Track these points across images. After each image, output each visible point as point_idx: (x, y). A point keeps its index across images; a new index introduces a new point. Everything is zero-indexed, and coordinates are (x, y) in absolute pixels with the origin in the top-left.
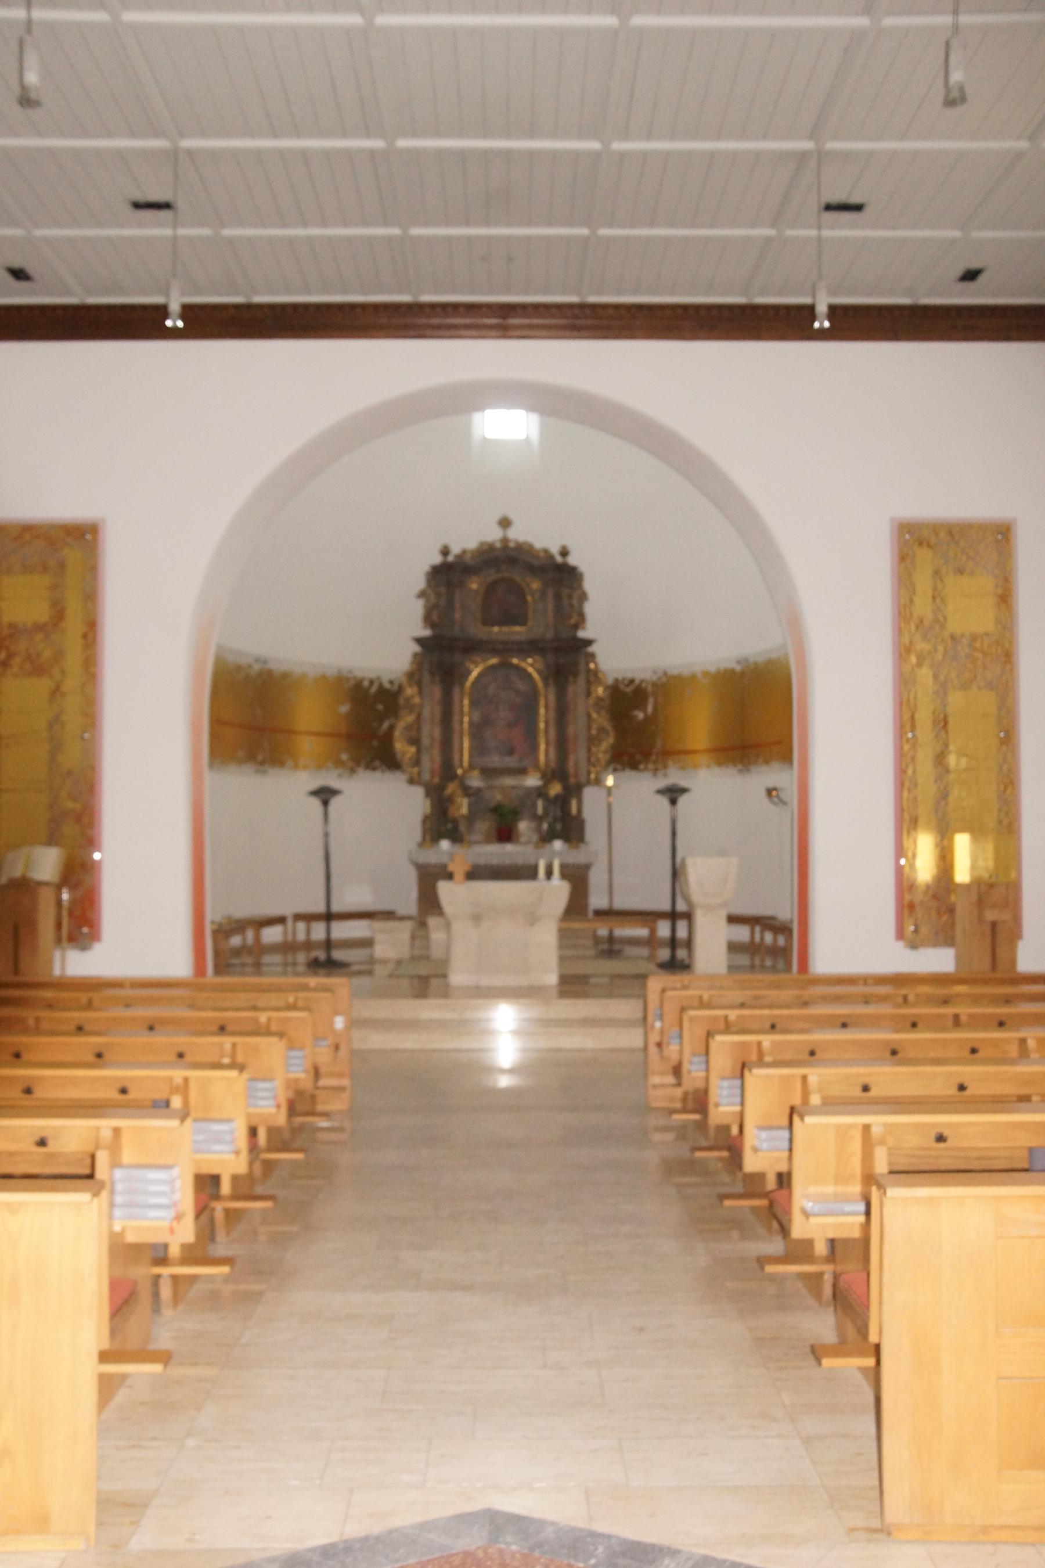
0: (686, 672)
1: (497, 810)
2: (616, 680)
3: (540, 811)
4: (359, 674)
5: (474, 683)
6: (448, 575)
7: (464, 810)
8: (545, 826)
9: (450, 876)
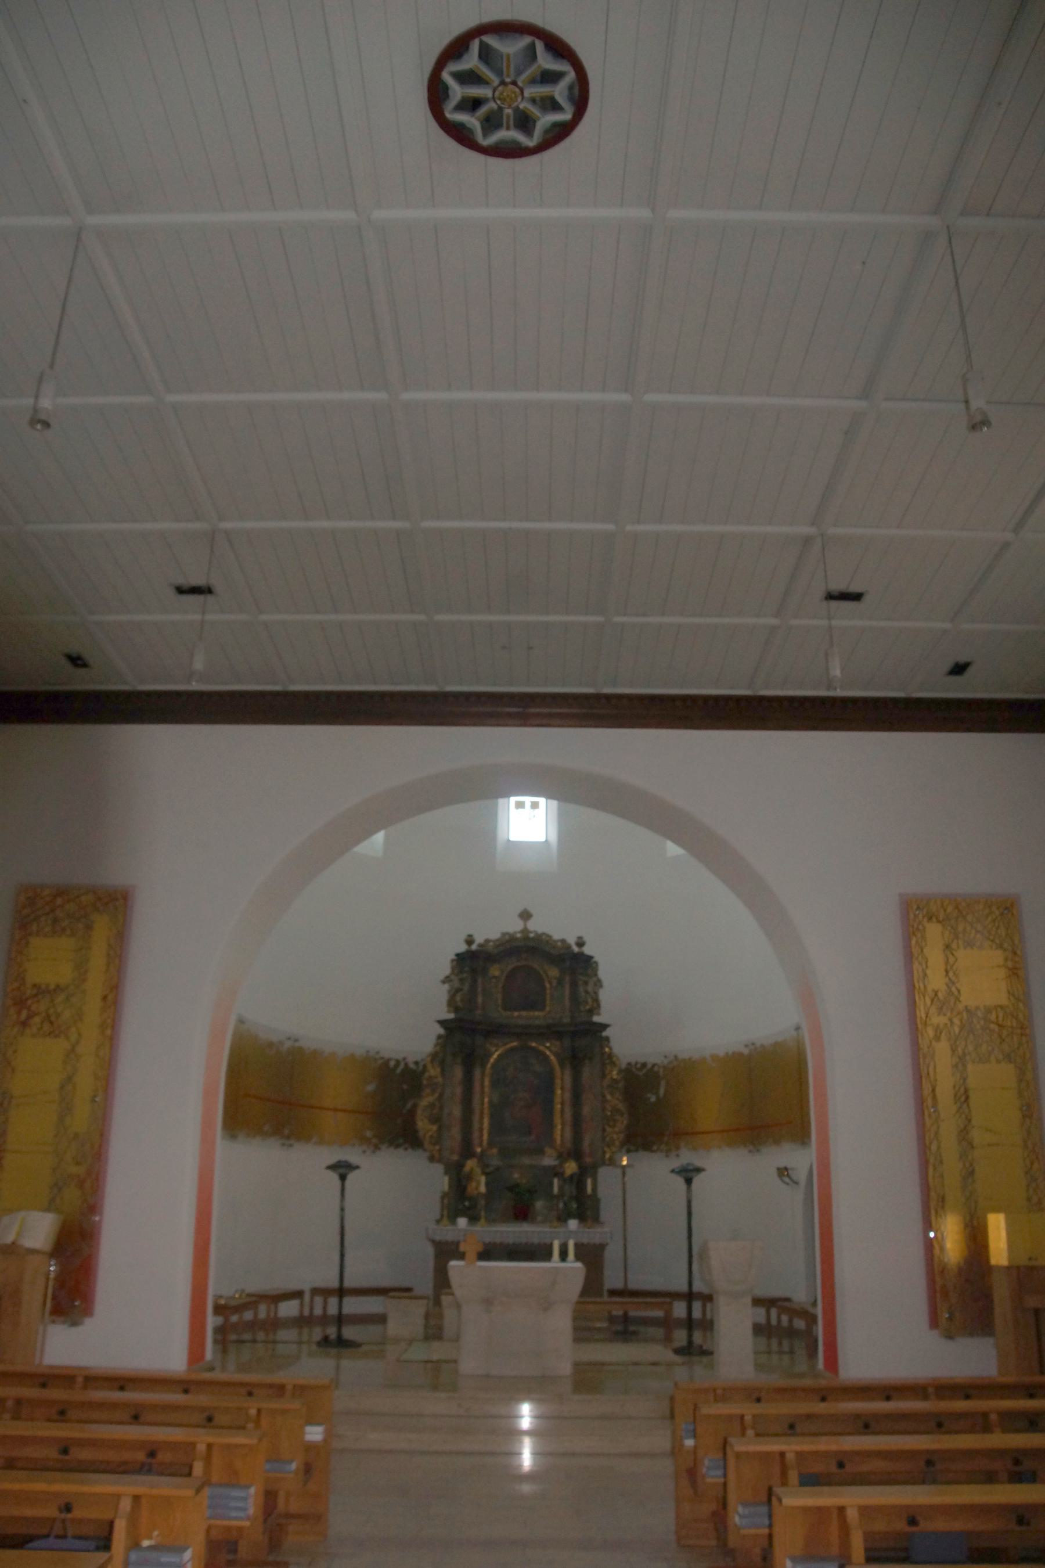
1: (513, 1188)
2: (629, 1064)
3: (556, 1190)
4: (386, 1055)
5: (494, 1066)
6: (472, 962)
7: (483, 1189)
8: (561, 1205)
9: (462, 1256)
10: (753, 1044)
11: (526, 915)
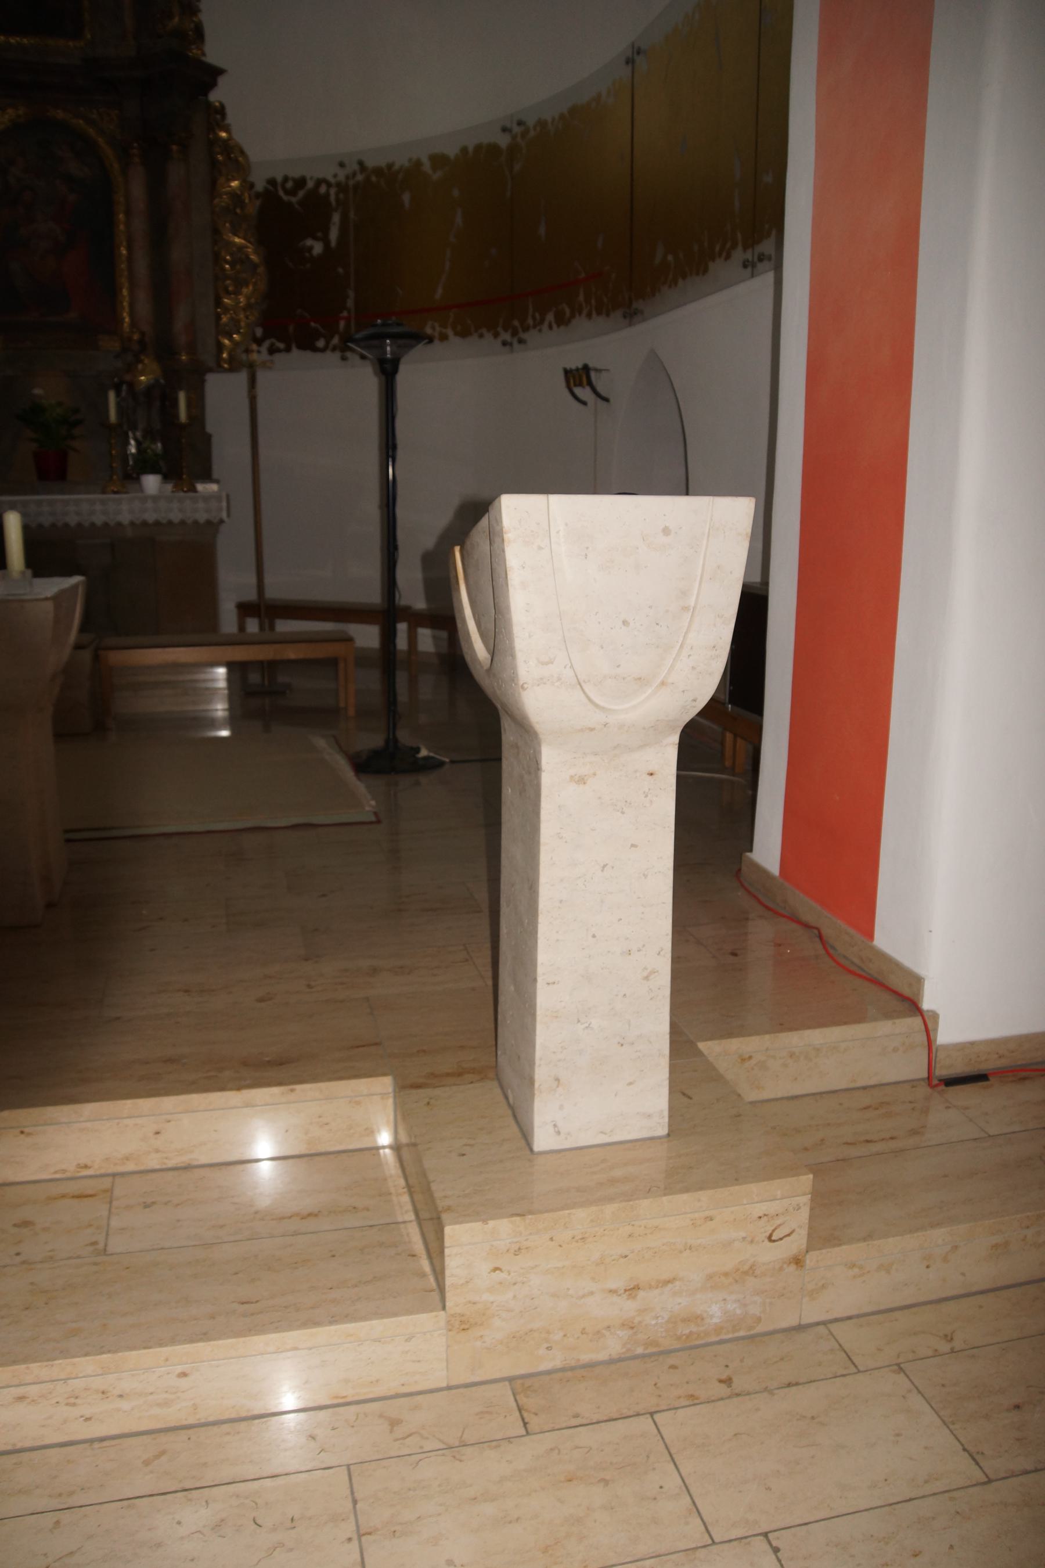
0: (401, 161)
2: (272, 182)
10: (520, 123)
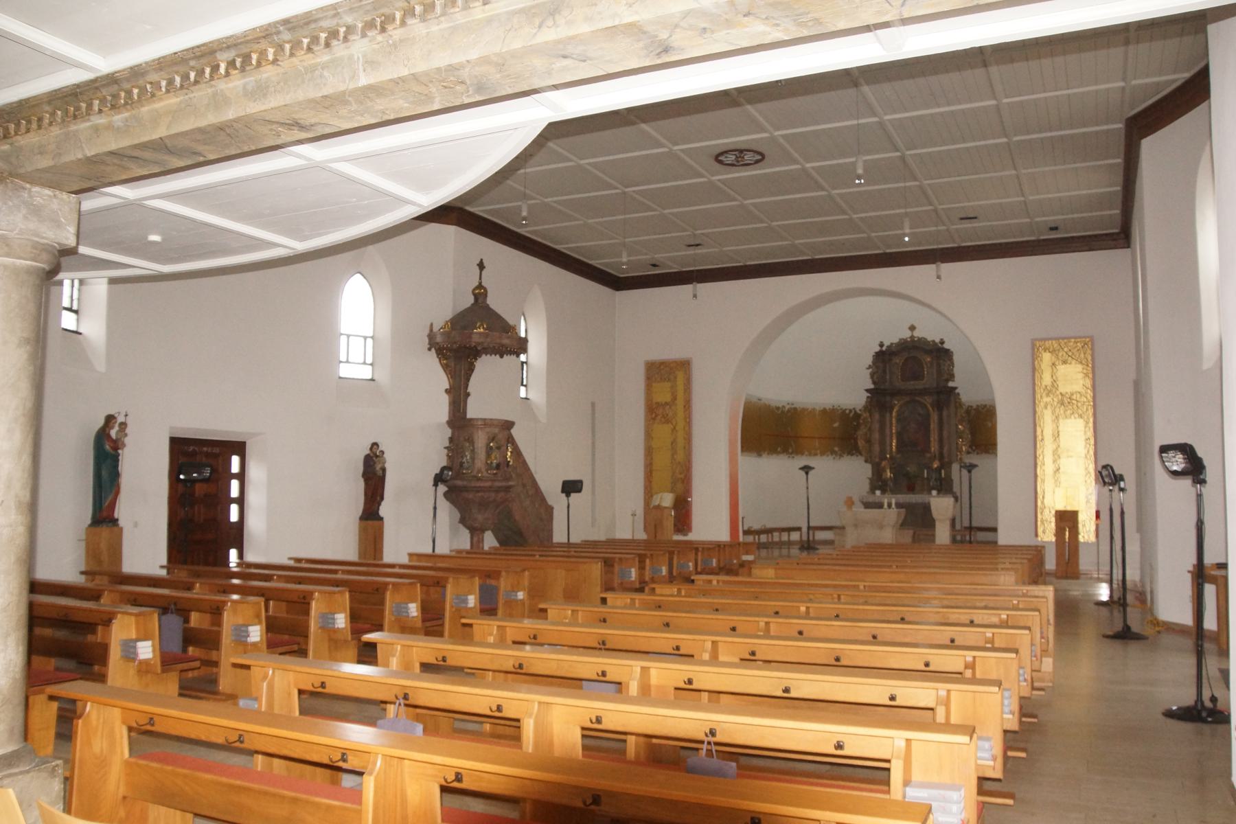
6: (883, 357)
11: (912, 328)
